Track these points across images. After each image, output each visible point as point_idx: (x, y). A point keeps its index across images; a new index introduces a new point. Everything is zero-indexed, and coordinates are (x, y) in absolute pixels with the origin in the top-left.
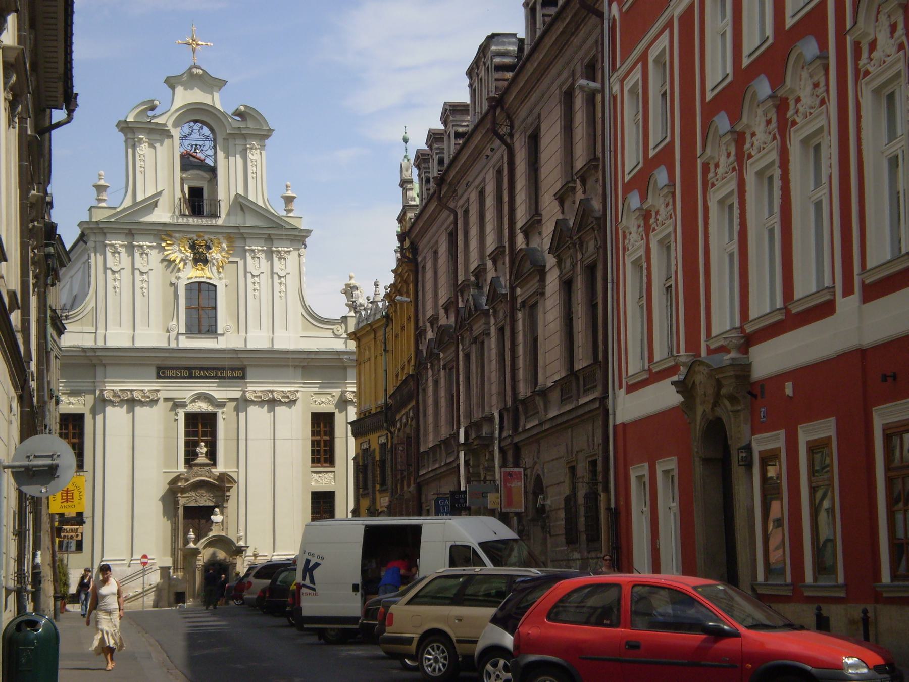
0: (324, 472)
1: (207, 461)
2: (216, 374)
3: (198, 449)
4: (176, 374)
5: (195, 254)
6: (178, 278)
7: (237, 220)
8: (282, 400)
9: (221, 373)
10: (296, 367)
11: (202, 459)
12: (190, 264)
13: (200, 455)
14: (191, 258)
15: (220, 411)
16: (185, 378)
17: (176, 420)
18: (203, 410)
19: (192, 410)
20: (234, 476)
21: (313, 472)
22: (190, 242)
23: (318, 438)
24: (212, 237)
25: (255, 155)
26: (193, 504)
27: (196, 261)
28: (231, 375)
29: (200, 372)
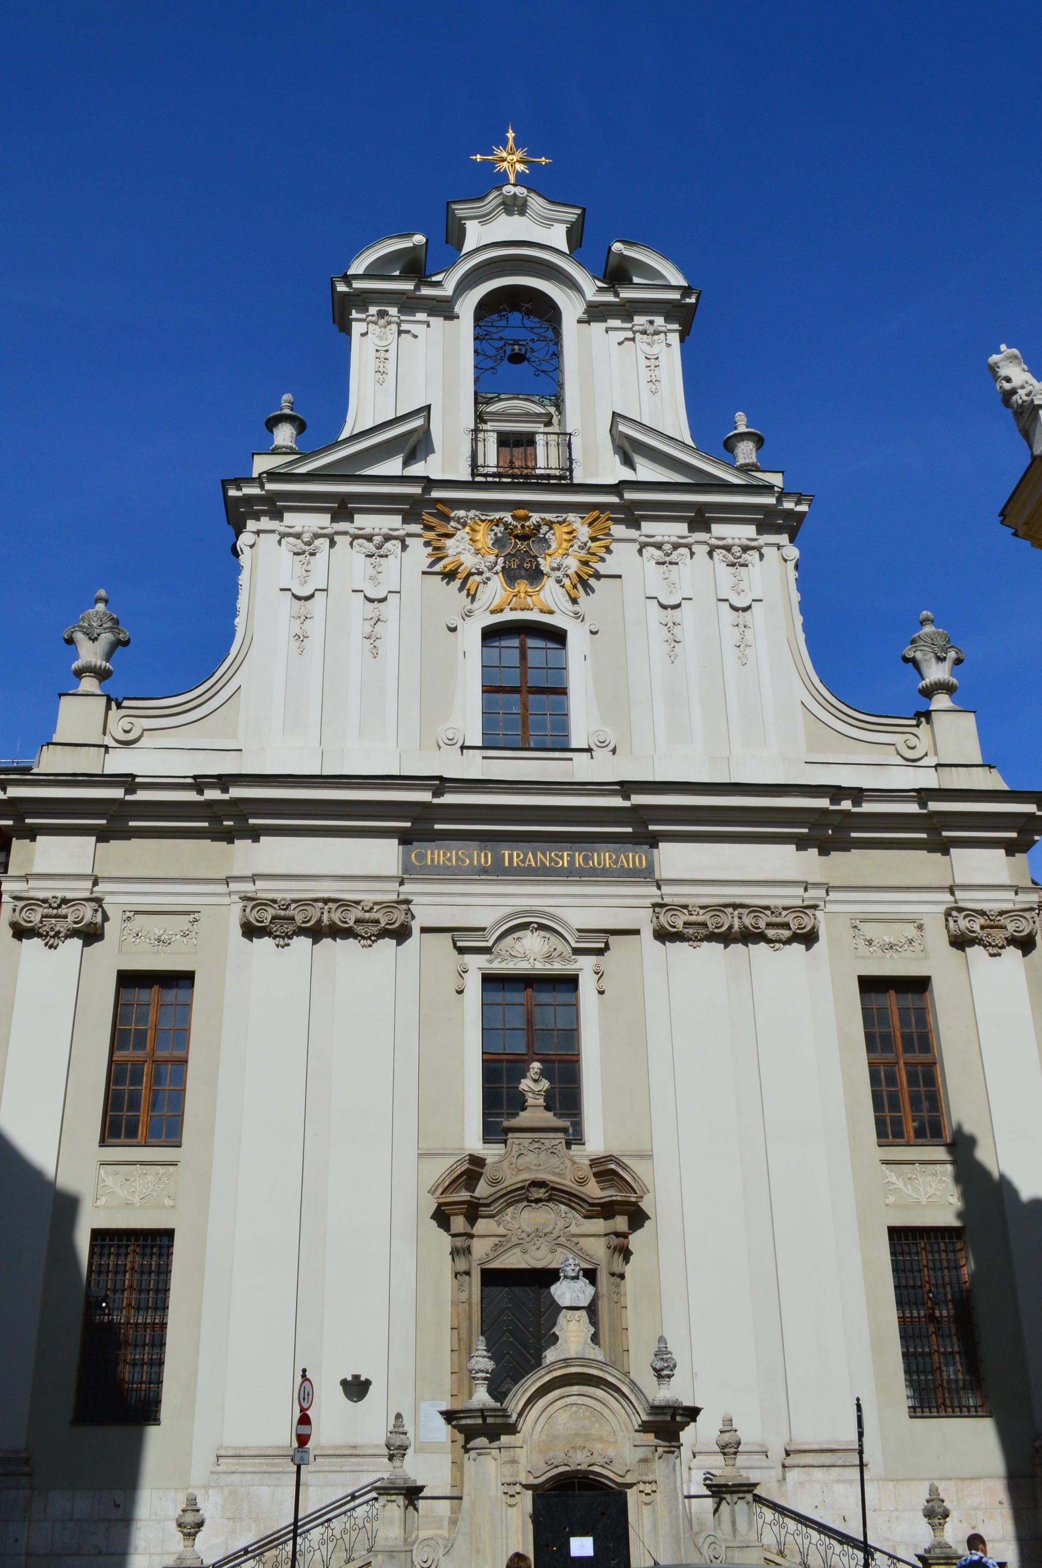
1: (549, 1118)
2: (571, 862)
3: (525, 1084)
4: (458, 858)
6: (469, 614)
7: (615, 472)
8: (771, 933)
9: (586, 859)
11: (535, 1114)
12: (497, 582)
13: (530, 1101)
14: (498, 568)
15: (585, 965)
16: (485, 871)
18: (538, 965)
19: (503, 965)
21: (886, 1162)
23: (889, 1057)
24: (550, 516)
25: (656, 346)
27: (510, 576)
28: (616, 862)
29: (525, 855)
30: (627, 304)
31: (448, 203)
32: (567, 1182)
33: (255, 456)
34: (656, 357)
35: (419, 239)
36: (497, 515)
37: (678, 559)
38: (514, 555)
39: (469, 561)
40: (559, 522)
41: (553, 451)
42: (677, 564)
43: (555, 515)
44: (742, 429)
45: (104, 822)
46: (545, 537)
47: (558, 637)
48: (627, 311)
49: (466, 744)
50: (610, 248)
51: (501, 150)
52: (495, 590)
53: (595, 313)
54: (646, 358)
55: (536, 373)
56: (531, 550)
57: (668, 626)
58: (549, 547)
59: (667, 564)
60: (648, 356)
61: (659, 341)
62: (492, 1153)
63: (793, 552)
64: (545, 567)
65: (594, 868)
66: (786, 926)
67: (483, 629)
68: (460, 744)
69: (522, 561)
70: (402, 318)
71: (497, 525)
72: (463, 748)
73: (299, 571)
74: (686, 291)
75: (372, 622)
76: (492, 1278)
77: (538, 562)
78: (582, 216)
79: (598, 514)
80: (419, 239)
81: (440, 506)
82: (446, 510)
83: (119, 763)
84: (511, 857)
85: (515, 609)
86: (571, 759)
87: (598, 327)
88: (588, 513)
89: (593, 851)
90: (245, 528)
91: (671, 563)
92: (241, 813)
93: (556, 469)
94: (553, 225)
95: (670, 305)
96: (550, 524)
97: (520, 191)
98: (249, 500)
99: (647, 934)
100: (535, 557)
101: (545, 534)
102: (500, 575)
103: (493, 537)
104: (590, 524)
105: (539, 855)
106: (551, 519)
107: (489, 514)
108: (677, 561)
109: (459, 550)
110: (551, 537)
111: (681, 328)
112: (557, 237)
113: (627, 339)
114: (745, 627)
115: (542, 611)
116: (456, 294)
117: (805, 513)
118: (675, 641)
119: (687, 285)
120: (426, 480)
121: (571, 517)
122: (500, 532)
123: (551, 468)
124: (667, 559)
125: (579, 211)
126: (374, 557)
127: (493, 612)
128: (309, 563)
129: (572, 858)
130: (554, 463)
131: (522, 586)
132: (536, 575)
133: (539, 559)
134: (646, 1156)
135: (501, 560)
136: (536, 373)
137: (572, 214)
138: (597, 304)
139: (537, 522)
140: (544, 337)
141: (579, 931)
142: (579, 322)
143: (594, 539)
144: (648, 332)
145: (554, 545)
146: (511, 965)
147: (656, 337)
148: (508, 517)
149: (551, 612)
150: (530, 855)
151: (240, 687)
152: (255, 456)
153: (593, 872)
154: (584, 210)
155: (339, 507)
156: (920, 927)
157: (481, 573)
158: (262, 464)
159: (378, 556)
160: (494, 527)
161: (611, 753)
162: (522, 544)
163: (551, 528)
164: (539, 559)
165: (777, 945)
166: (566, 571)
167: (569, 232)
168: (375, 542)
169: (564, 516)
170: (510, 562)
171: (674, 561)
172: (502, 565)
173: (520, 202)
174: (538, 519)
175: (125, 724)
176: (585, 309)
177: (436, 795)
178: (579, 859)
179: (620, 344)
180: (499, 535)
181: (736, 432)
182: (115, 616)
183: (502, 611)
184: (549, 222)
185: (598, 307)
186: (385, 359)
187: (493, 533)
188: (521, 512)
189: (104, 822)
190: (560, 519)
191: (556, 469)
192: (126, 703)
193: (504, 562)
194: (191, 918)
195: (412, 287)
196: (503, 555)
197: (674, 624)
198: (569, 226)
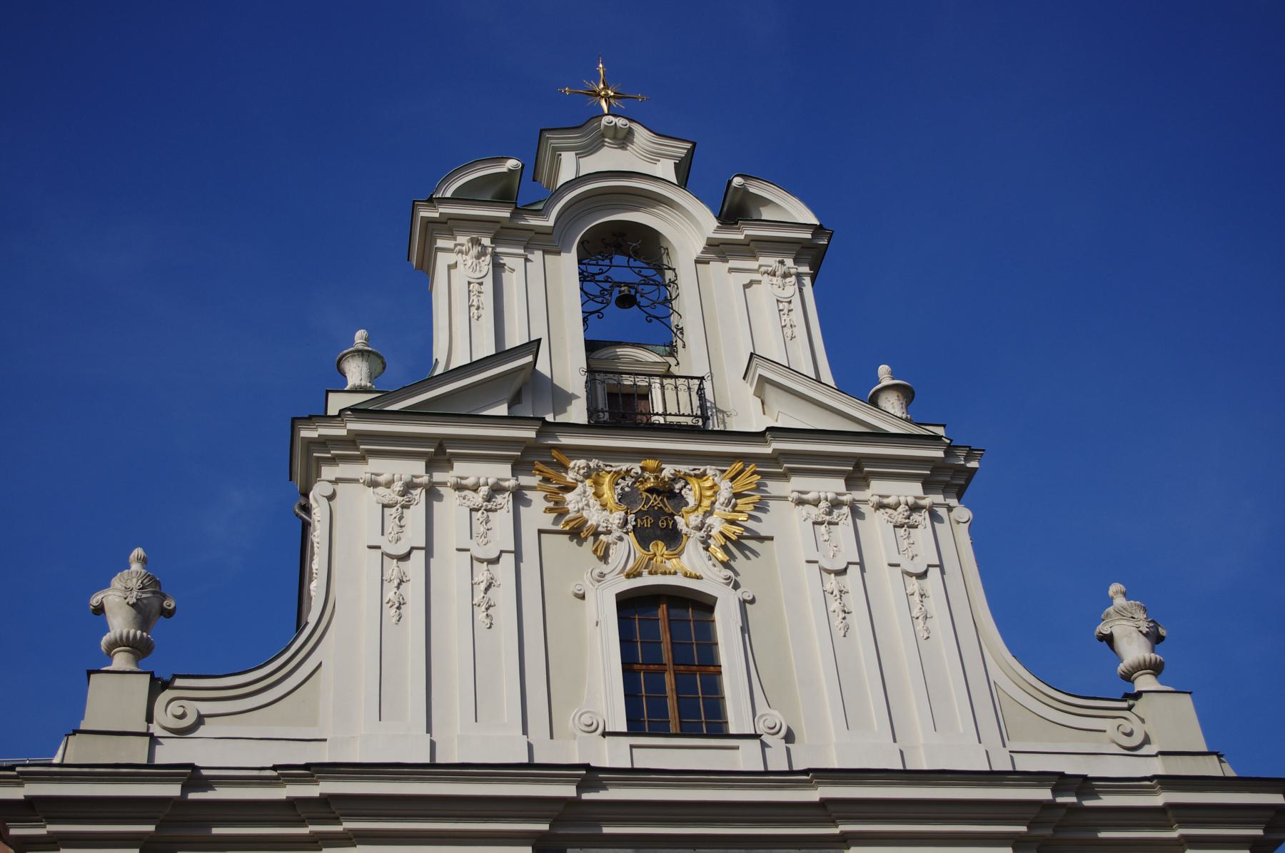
5: (639, 515)
14: (630, 527)
22: (623, 483)
24: (684, 469)
30: (752, 244)
31: (542, 131)
33: (330, 395)
34: (789, 299)
35: (512, 163)
36: (624, 466)
37: (839, 519)
39: (595, 517)
40: (696, 476)
41: (684, 396)
42: (837, 524)
43: (692, 467)
44: (886, 381)
45: (151, 828)
46: (680, 492)
47: (705, 605)
48: (751, 248)
49: (607, 730)
50: (730, 182)
51: (592, 84)
52: (625, 549)
53: (718, 250)
54: (778, 301)
55: (649, 319)
56: (666, 507)
57: (834, 594)
59: (826, 524)
60: (780, 299)
61: (790, 284)
63: (963, 513)
67: (617, 595)
68: (600, 730)
69: (657, 519)
70: (499, 250)
71: (623, 478)
72: (605, 734)
73: (391, 525)
74: (818, 230)
75: (483, 586)
77: (675, 521)
78: (691, 152)
79: (742, 467)
80: (512, 163)
81: (554, 453)
82: (562, 458)
83: (170, 752)
85: (656, 573)
86: (737, 748)
87: (717, 269)
88: (730, 466)
90: (320, 477)
91: (830, 523)
92: (332, 815)
93: (689, 416)
94: (659, 161)
95: (800, 245)
96: (685, 478)
97: (620, 122)
98: (324, 442)
100: (672, 515)
101: (681, 490)
102: (631, 534)
103: (620, 492)
104: (732, 479)
106: (687, 471)
107: (613, 464)
108: (837, 521)
109: (580, 505)
110: (688, 492)
111: (812, 272)
112: (666, 169)
113: (751, 283)
114: (922, 596)
115: (686, 575)
116: (557, 225)
117: (976, 469)
118: (845, 612)
119: (818, 224)
120: (540, 423)
121: (710, 470)
122: (628, 486)
123: (683, 415)
124: (828, 518)
125: (689, 146)
126: (480, 512)
127: (628, 576)
128: (401, 518)
130: (685, 409)
131: (659, 548)
132: (673, 538)
133: (676, 517)
135: (631, 517)
136: (649, 319)
137: (681, 149)
138: (717, 243)
139: (671, 474)
140: (652, 280)
142: (697, 262)
143: (738, 495)
144: (777, 274)
145: (692, 501)
147: (788, 280)
148: (636, 468)
149: (698, 578)
151: (320, 664)
152: (330, 395)
154: (694, 144)
155: (436, 453)
157: (609, 532)
158: (337, 403)
159: (485, 510)
160: (620, 481)
161: (783, 741)
162: (655, 499)
163: (687, 483)
164: (676, 517)
166: (710, 531)
167: (677, 166)
168: (481, 494)
169: (702, 468)
170: (642, 520)
171: (833, 520)
172: (634, 523)
173: (621, 135)
174: (673, 472)
175: (175, 708)
176: (704, 248)
179: (746, 286)
180: (627, 489)
181: (879, 386)
182: (158, 579)
183: (640, 575)
184: (656, 157)
185: (718, 246)
186: (479, 292)
187: (619, 487)
188: (651, 463)
189: (151, 828)
191: (689, 416)
192: (178, 682)
193: (636, 520)
195: (508, 215)
196: (634, 512)
197: (841, 591)
198: (677, 162)
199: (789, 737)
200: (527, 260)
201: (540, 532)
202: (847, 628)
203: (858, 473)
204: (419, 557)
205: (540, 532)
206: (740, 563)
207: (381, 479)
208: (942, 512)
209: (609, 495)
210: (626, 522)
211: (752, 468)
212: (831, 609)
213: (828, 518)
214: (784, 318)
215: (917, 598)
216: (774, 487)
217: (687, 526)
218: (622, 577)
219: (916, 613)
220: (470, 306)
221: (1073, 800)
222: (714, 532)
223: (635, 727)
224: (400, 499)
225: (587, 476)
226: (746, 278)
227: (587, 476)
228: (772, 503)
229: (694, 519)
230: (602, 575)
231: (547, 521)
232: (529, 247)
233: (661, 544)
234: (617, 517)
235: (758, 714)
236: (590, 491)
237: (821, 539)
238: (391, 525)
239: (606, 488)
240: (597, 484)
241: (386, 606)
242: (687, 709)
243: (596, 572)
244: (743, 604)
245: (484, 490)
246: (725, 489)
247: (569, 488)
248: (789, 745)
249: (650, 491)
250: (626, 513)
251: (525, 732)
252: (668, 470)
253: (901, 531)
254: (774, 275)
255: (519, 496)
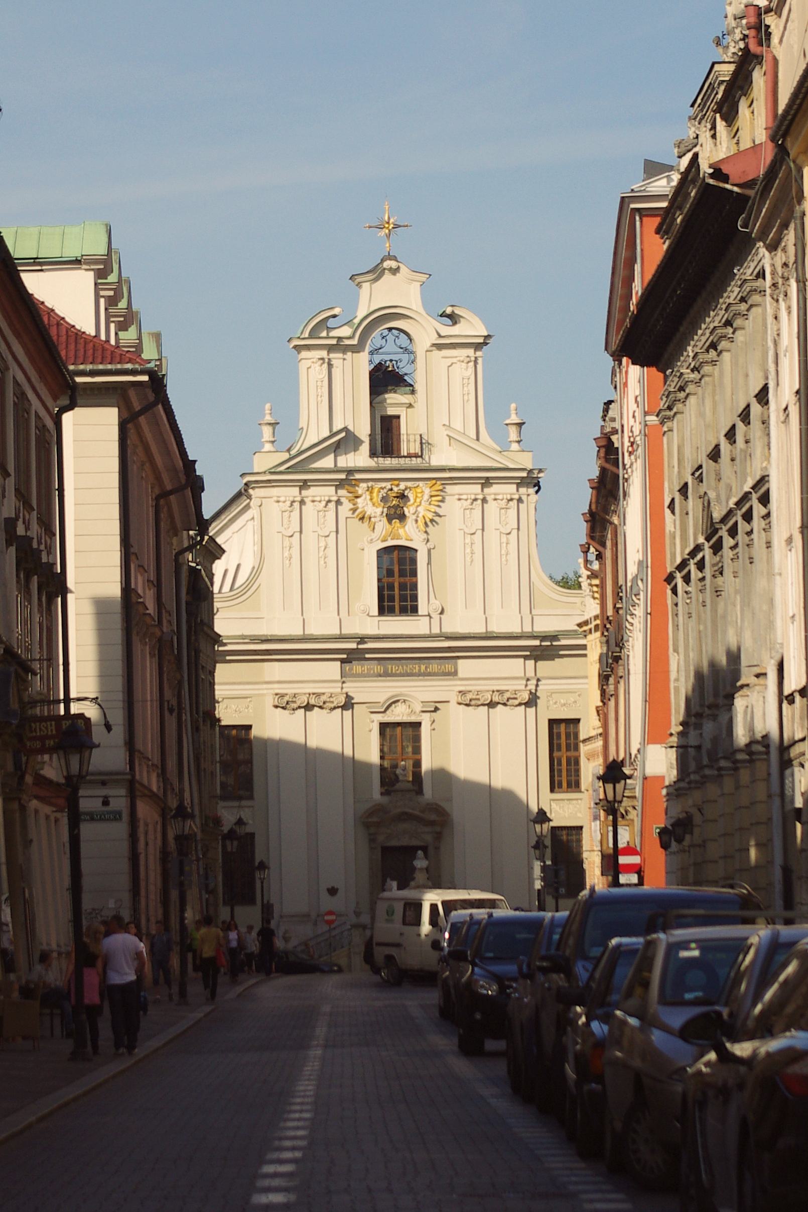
0: (568, 800)
5: (389, 508)
9: (426, 668)
10: (526, 658)
14: (384, 514)
17: (370, 731)
19: (389, 718)
20: (443, 804)
24: (409, 484)
26: (394, 843)
27: (390, 518)
32: (417, 813)
36: (383, 484)
38: (392, 507)
52: (382, 525)
58: (409, 501)
62: (385, 800)
64: (406, 513)
65: (430, 673)
66: (515, 698)
67: (378, 551)
75: (323, 548)
76: (386, 850)
84: (392, 668)
89: (429, 664)
96: (410, 488)
99: (453, 703)
105: (405, 667)
115: (407, 540)
121: (421, 484)
124: (471, 507)
127: (383, 541)
129: (420, 667)
131: (396, 522)
132: (402, 517)
134: (449, 800)
135: (385, 510)
141: (422, 702)
143: (431, 496)
145: (412, 501)
146: (392, 718)
148: (388, 485)
149: (411, 540)
150: (400, 667)
153: (430, 674)
156: (579, 695)
165: (512, 707)
177: (358, 643)
178: (423, 667)
180: (385, 495)
183: (387, 540)
188: (396, 482)
190: (415, 485)
194: (249, 699)
199: (442, 613)
200: (344, 359)
201: (347, 518)
202: (472, 561)
203: (487, 483)
204: (297, 535)
205: (347, 518)
206: (431, 529)
207: (282, 499)
208: (524, 498)
209: (377, 497)
210: (383, 512)
211: (439, 483)
212: (466, 552)
213: (471, 507)
214: (465, 389)
215: (504, 545)
216: (449, 489)
217: (409, 512)
218: (379, 541)
219: (503, 552)
220: (317, 396)
221: (549, 643)
222: (421, 515)
223: (382, 611)
224: (289, 509)
225: (368, 490)
226: (449, 361)
227: (368, 490)
228: (447, 498)
229: (412, 509)
230: (372, 540)
231: (350, 514)
232: (344, 352)
233: (397, 521)
234: (379, 510)
235: (431, 602)
236: (368, 497)
237: (466, 517)
238: (285, 521)
239: (375, 495)
240: (371, 493)
241: (285, 559)
242: (403, 598)
243: (369, 539)
244: (429, 551)
245: (324, 503)
246: (427, 491)
247: (357, 497)
248: (442, 616)
249: (395, 497)
250: (383, 507)
251: (338, 614)
252: (402, 486)
253: (503, 511)
254: (463, 362)
255: (338, 503)
